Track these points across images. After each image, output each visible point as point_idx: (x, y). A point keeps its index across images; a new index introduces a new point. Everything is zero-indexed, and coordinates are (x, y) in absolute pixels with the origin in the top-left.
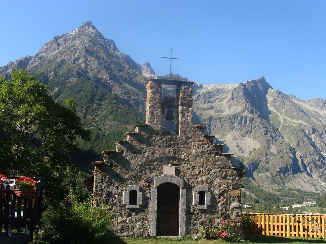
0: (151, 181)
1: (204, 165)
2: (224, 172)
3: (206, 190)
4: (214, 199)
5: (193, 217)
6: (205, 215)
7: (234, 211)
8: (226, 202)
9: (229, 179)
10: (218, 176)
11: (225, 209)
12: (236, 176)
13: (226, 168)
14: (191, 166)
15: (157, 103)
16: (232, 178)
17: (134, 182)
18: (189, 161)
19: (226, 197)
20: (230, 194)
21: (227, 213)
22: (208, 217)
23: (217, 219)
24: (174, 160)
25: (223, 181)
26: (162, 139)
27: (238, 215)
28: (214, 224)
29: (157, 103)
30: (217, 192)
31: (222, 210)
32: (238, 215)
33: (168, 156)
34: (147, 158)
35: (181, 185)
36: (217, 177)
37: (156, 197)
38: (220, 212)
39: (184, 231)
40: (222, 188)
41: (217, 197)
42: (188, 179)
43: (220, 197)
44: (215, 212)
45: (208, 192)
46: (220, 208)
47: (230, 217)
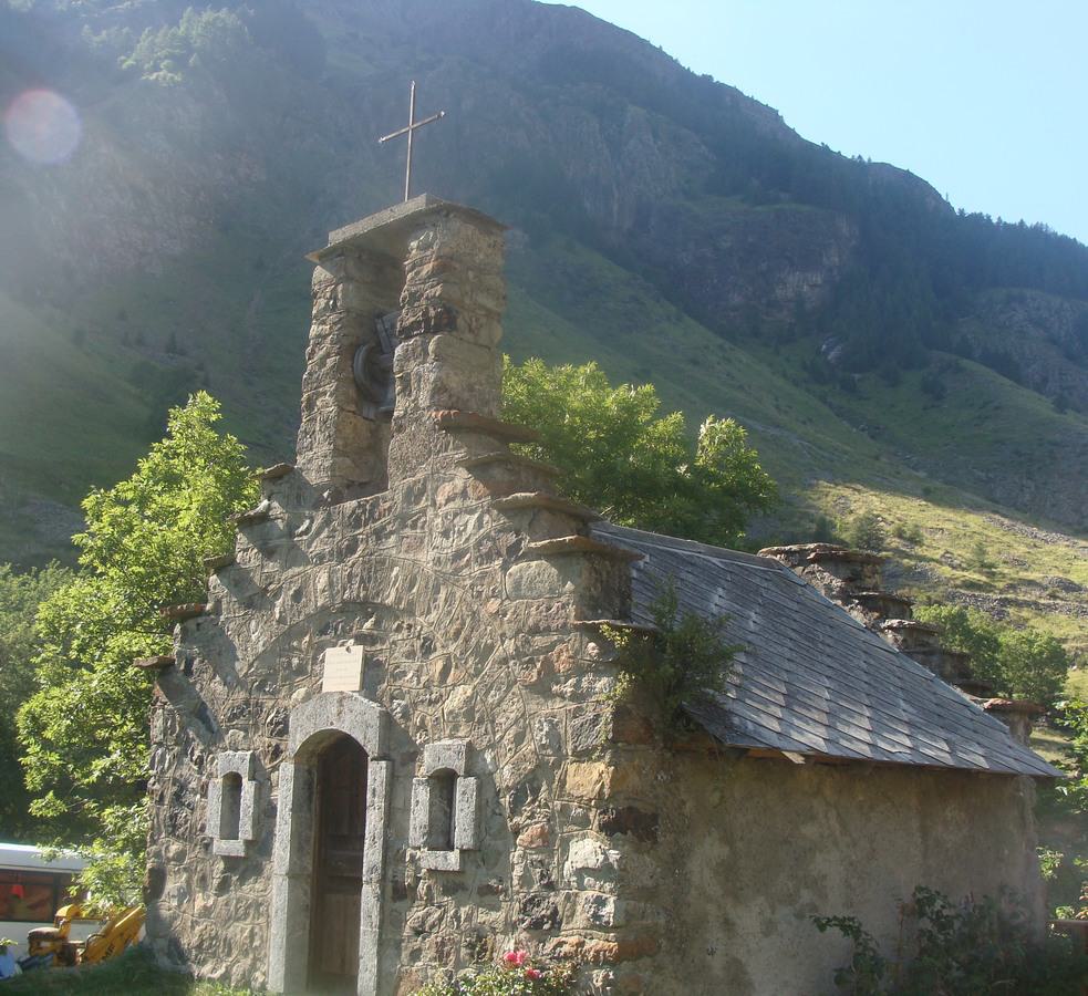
0: (281, 728)
1: (463, 624)
2: (538, 652)
3: (459, 764)
4: (494, 813)
5: (415, 914)
6: (458, 907)
7: (585, 889)
8: (542, 835)
9: (562, 696)
10: (516, 682)
11: (542, 876)
12: (598, 673)
13: (548, 630)
14: (418, 637)
15: (328, 355)
16: (577, 685)
17: (242, 734)
18: (414, 615)
19: (546, 806)
20: (563, 783)
21: (551, 900)
22: (469, 918)
23: (505, 933)
24: (356, 613)
25: (533, 707)
26: (327, 522)
27: (596, 916)
28: (491, 959)
29: (328, 355)
30: (506, 776)
31: (526, 880)
32: (596, 916)
33: (343, 601)
34: (279, 622)
35: (370, 743)
36: (510, 687)
37: (290, 806)
38: (518, 893)
39: (372, 984)
40: (528, 747)
41: (506, 800)
42: (406, 706)
43: (522, 803)
44: (496, 892)
45: (468, 774)
46: (518, 872)
47: (564, 926)
